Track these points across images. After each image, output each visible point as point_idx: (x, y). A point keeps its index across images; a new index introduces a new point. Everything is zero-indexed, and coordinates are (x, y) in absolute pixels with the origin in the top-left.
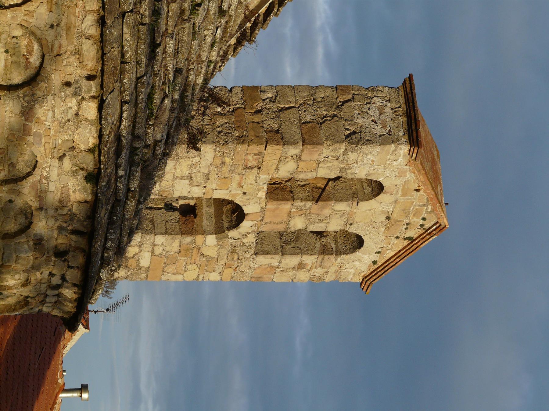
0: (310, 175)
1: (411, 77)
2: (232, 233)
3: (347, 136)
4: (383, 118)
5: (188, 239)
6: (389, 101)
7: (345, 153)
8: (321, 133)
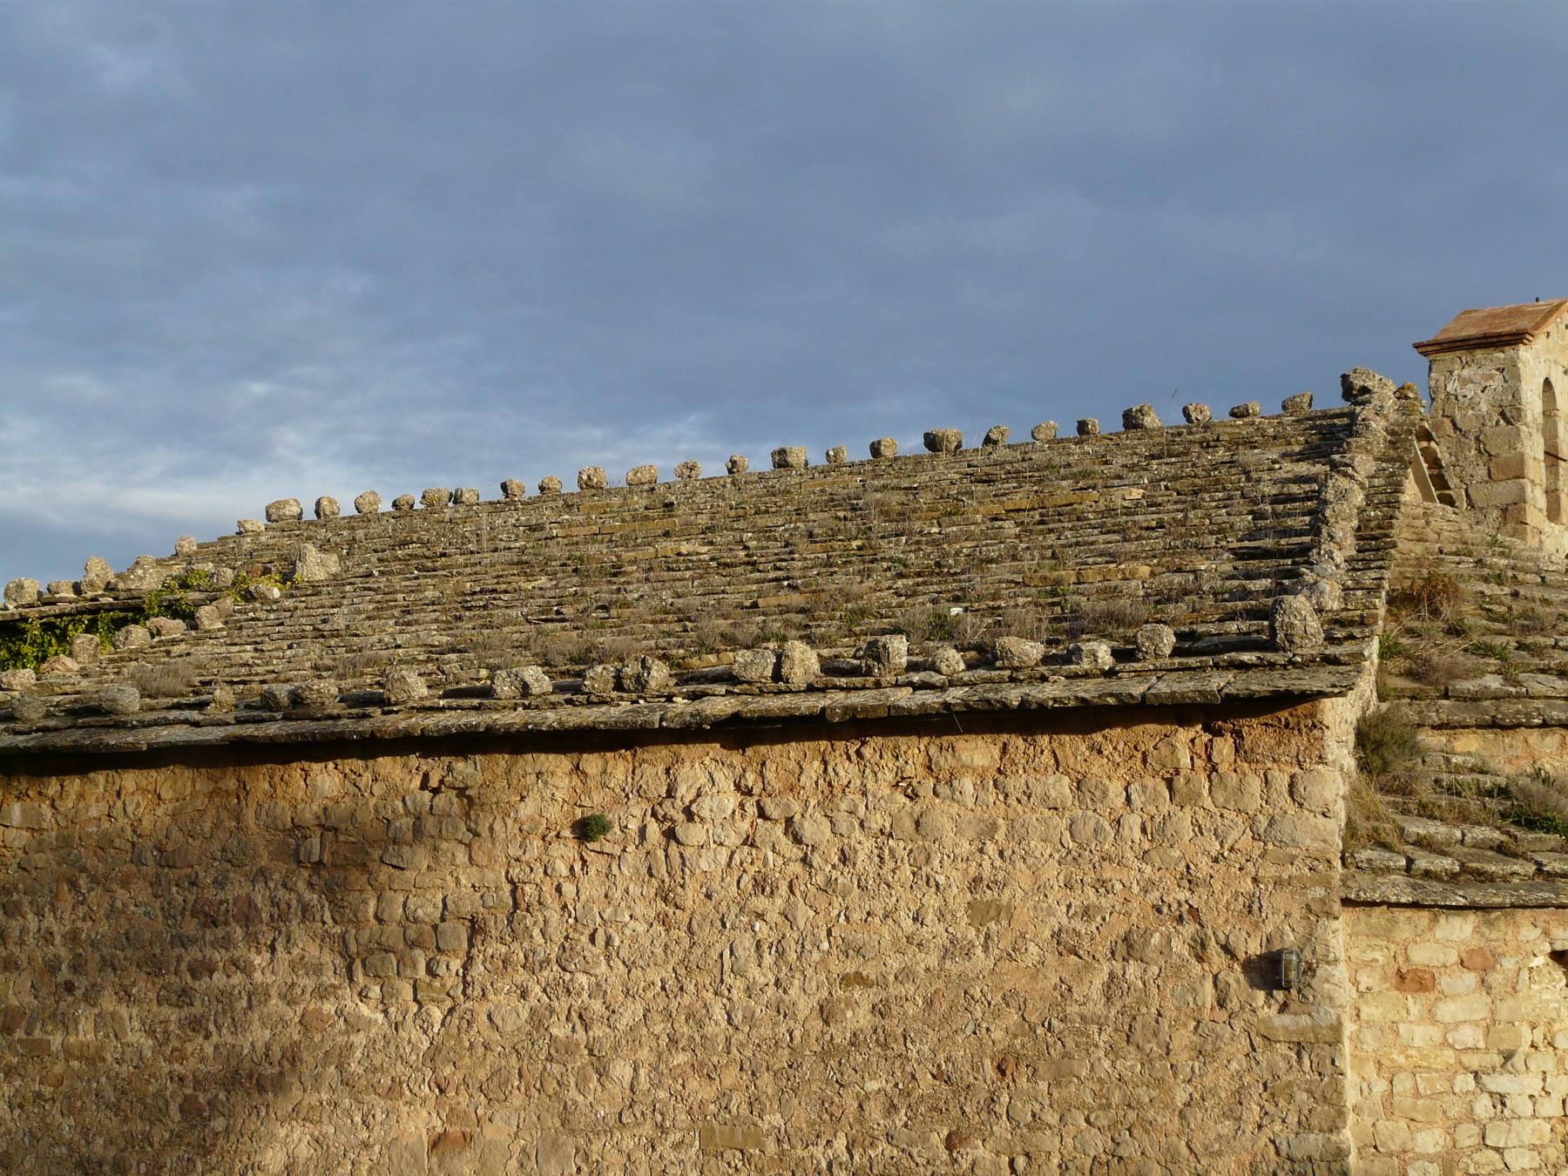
1: (1417, 346)
3: (1508, 422)
6: (1451, 373)
7: (1526, 424)
8: (1504, 455)
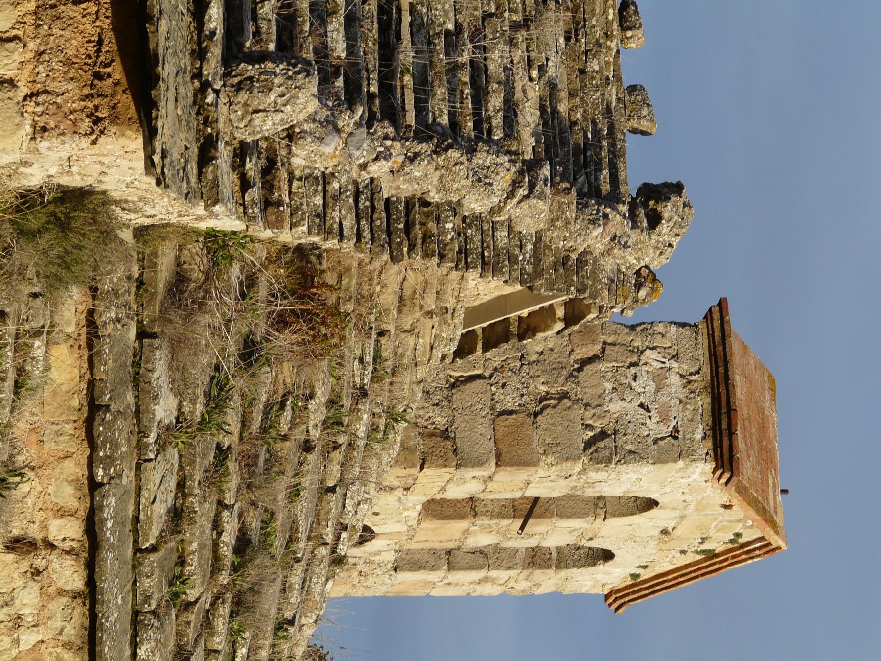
1: (722, 305)
3: (589, 444)
4: (663, 398)
6: (675, 357)
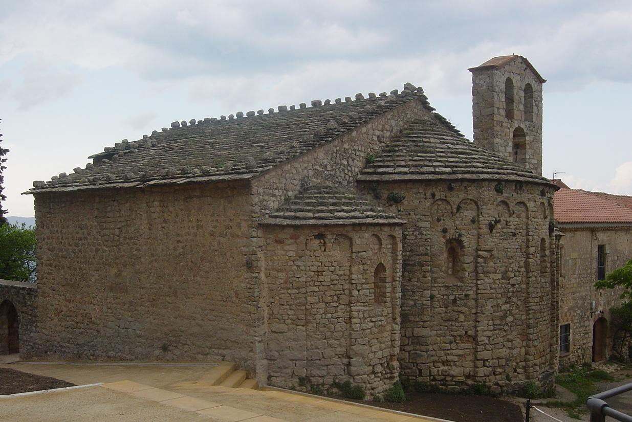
0: (504, 104)
2: (525, 131)
5: (527, 146)
